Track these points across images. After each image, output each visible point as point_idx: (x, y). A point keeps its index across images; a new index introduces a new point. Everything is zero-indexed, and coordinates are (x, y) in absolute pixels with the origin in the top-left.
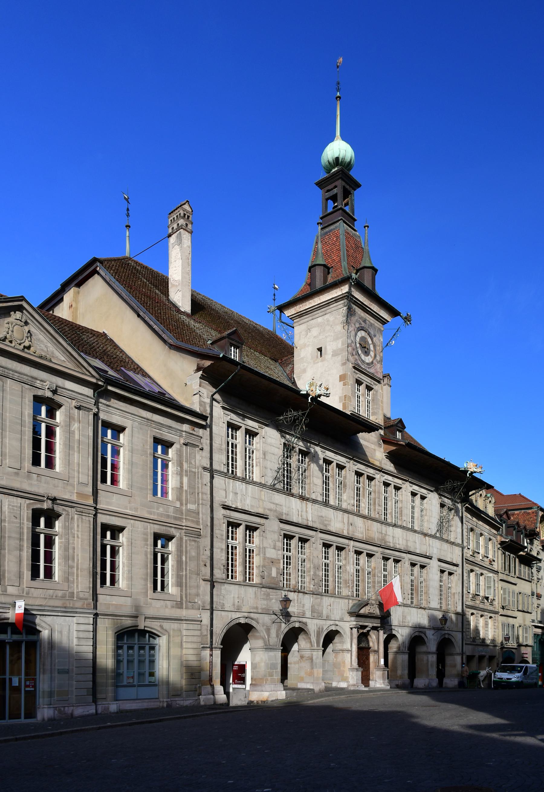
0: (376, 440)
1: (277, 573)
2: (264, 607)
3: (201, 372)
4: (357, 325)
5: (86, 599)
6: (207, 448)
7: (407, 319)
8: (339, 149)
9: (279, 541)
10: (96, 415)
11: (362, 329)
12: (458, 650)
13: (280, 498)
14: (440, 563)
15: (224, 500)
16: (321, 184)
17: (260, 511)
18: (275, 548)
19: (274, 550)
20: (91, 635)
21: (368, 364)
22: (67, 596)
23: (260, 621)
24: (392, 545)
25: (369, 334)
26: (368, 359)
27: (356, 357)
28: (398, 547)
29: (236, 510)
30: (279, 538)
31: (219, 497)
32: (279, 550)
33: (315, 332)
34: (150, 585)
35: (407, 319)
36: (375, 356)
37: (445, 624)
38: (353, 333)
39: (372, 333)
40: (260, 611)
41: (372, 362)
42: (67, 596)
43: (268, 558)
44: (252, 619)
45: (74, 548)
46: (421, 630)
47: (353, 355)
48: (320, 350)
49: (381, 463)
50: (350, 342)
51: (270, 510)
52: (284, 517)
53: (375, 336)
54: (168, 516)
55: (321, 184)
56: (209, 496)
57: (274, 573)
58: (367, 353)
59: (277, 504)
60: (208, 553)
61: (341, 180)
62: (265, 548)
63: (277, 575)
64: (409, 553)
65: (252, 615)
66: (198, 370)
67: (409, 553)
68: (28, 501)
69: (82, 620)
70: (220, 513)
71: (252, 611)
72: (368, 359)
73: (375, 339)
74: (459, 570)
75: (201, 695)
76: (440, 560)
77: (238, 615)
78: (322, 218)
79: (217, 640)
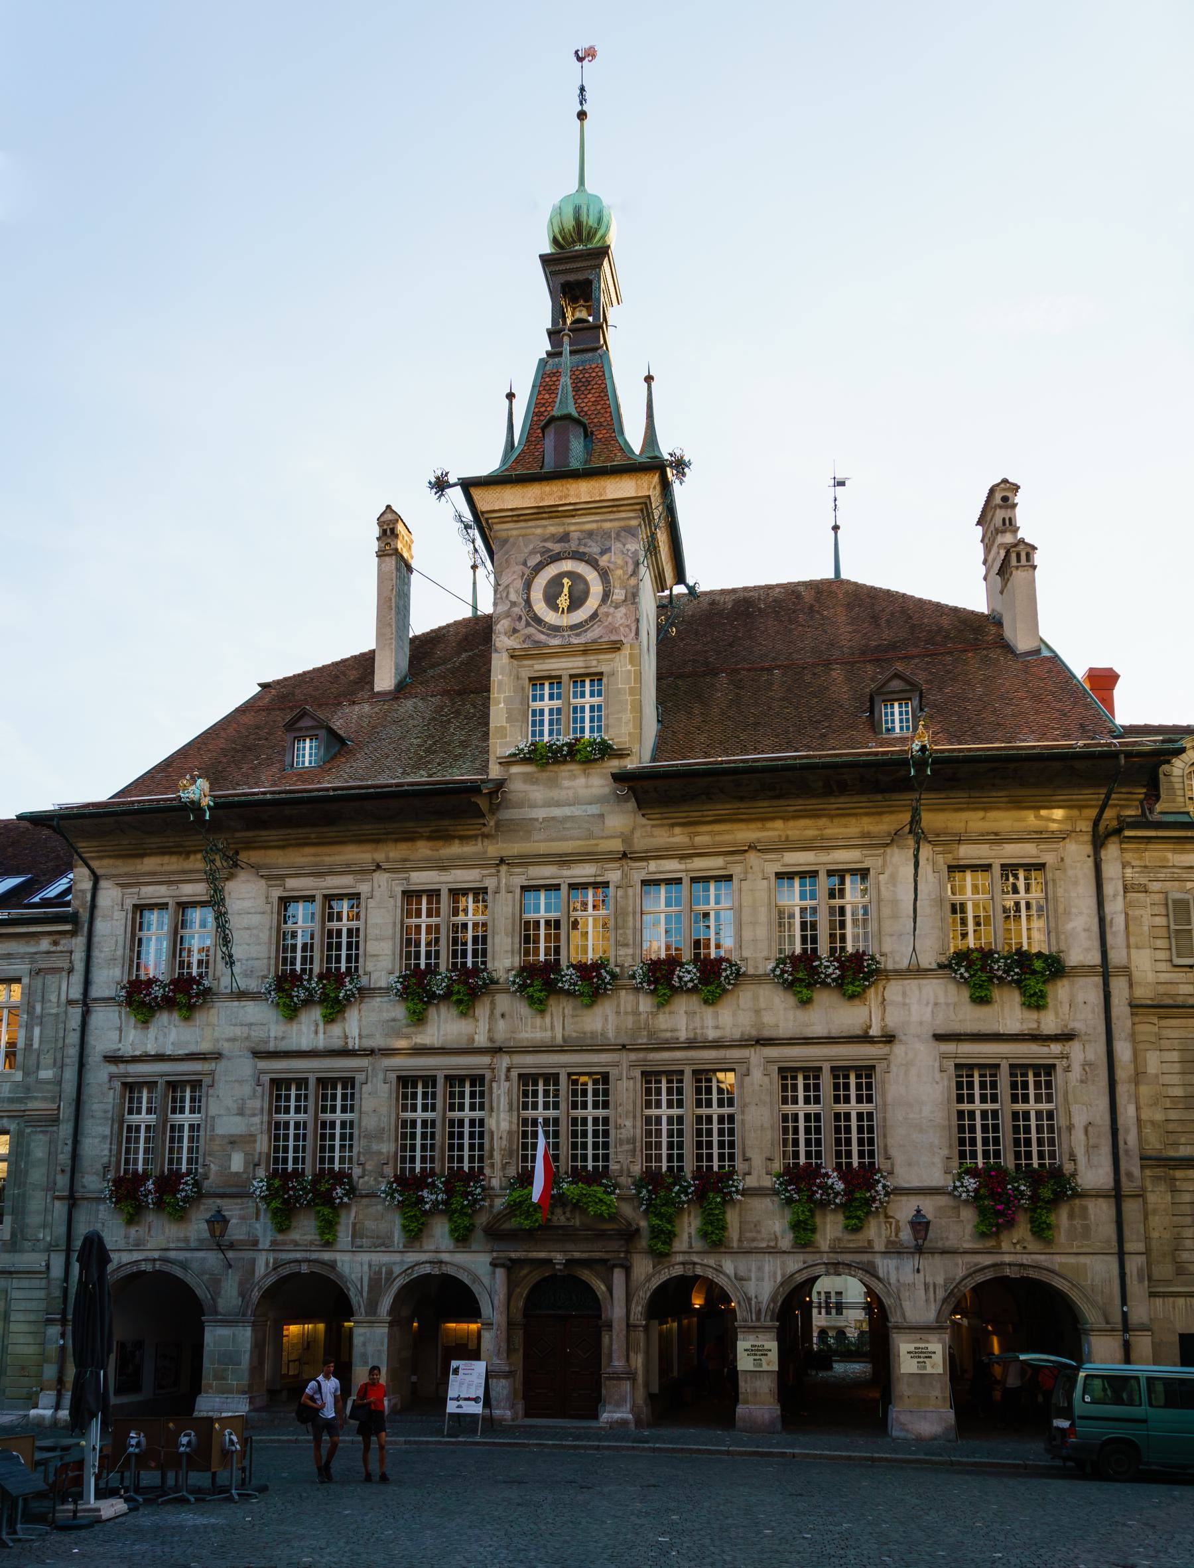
1: (246, 1163)
9: (254, 1096)
18: (241, 1113)
19: (238, 1119)
23: (195, 1265)
30: (254, 1091)
32: (254, 1115)
40: (193, 1245)
43: (223, 1136)
57: (237, 1163)
62: (213, 1118)
63: (246, 1167)
65: (172, 1255)
70: (99, 1074)
71: (172, 1245)
77: (136, 1256)
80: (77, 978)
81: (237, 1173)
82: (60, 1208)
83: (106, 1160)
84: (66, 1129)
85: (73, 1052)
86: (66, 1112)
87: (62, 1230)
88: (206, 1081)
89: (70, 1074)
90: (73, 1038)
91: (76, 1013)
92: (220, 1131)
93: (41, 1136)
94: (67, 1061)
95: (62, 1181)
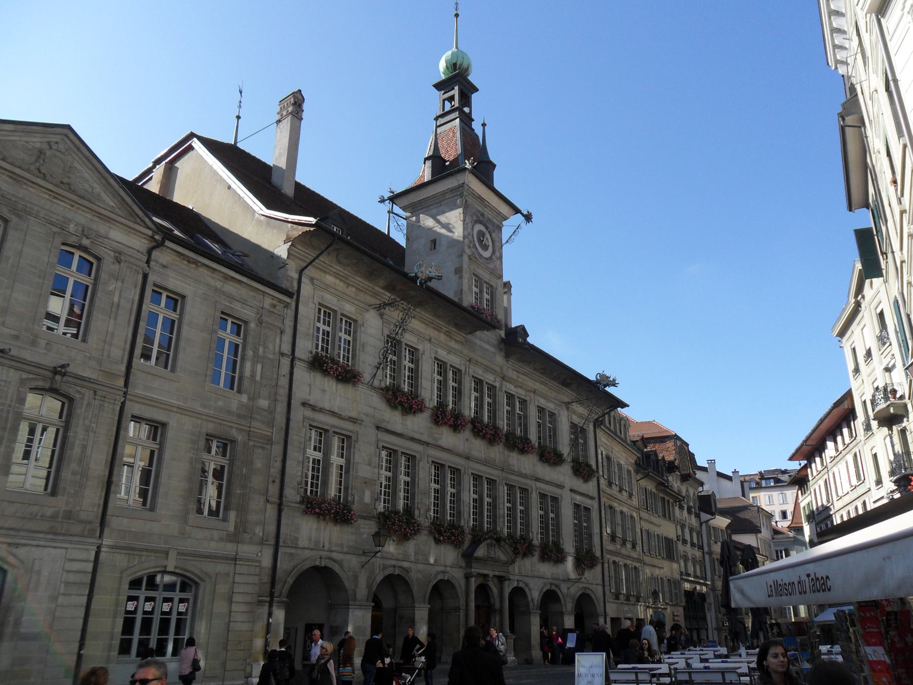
0: (496, 342)
2: (351, 544)
3: (290, 243)
4: (475, 218)
5: (90, 522)
6: (289, 332)
7: (528, 218)
10: (145, 277)
11: (480, 222)
12: (600, 609)
14: (573, 495)
15: (307, 397)
17: (354, 414)
18: (369, 465)
20: (88, 579)
21: (486, 259)
22: (61, 515)
24: (516, 469)
25: (487, 228)
26: (486, 254)
27: (474, 250)
28: (524, 471)
29: (322, 410)
31: (300, 393)
34: (193, 506)
35: (528, 218)
36: (494, 252)
37: (583, 574)
38: (470, 225)
39: (491, 227)
40: (345, 550)
41: (491, 258)
42: (61, 515)
44: (335, 561)
45: (84, 447)
46: (554, 582)
47: (469, 247)
49: (502, 369)
50: (466, 233)
51: (367, 415)
52: (383, 425)
53: (494, 231)
54: (229, 412)
56: (287, 391)
57: (367, 498)
58: (485, 248)
59: (375, 408)
60: (278, 465)
64: (537, 480)
67: (537, 480)
68: (25, 376)
69: (78, 555)
70: (298, 414)
72: (486, 254)
73: (493, 235)
74: (594, 505)
75: (251, 677)
76: (571, 490)
79: (283, 589)
80: (287, 337)
81: (367, 504)
82: (271, 511)
83: (299, 479)
84: (277, 449)
85: (283, 392)
86: (278, 436)
87: (272, 528)
88: (354, 437)
89: (281, 408)
90: (284, 382)
91: (286, 362)
92: (360, 474)
93: (260, 451)
94: (278, 397)
95: (274, 489)
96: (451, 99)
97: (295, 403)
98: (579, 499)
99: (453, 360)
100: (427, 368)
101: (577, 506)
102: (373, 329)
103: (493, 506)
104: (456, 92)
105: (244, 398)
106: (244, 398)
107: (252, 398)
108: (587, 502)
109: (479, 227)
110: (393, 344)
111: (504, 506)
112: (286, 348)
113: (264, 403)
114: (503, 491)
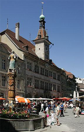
8: (42, 16)
13: (35, 74)
16: (40, 21)
26: (47, 51)
33: (39, 46)
35: (53, 45)
48: (39, 49)
55: (40, 21)
61: (43, 21)
66: (23, 53)
70: (26, 76)
76: (58, 84)
78: (40, 27)
89: (24, 75)
96: (42, 24)
97: (26, 75)
98: (58, 85)
99: (43, 67)
100: (40, 69)
101: (58, 86)
102: (33, 64)
103: (47, 86)
104: (42, 23)
105: (20, 75)
106: (20, 75)
107: (21, 74)
108: (59, 85)
109: (46, 47)
110: (36, 66)
111: (49, 86)
112: (24, 68)
113: (22, 75)
114: (49, 84)
